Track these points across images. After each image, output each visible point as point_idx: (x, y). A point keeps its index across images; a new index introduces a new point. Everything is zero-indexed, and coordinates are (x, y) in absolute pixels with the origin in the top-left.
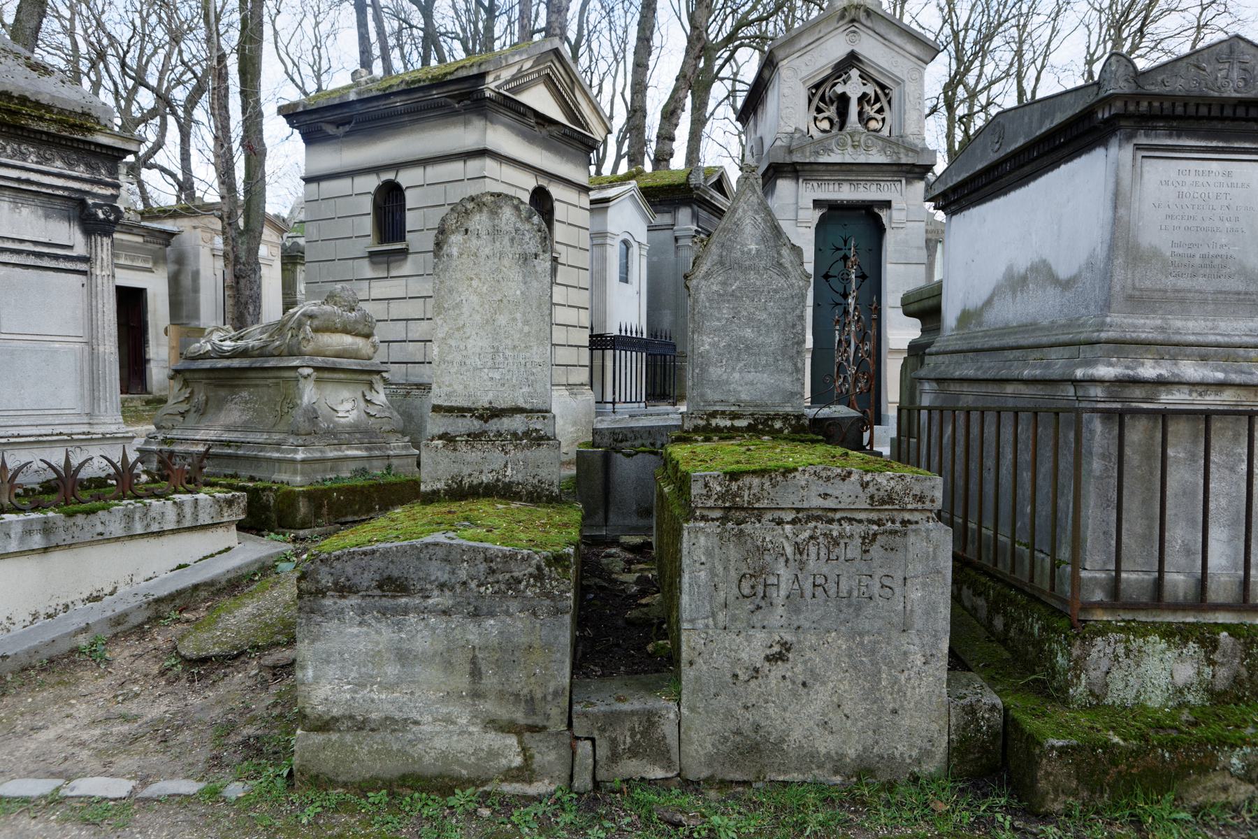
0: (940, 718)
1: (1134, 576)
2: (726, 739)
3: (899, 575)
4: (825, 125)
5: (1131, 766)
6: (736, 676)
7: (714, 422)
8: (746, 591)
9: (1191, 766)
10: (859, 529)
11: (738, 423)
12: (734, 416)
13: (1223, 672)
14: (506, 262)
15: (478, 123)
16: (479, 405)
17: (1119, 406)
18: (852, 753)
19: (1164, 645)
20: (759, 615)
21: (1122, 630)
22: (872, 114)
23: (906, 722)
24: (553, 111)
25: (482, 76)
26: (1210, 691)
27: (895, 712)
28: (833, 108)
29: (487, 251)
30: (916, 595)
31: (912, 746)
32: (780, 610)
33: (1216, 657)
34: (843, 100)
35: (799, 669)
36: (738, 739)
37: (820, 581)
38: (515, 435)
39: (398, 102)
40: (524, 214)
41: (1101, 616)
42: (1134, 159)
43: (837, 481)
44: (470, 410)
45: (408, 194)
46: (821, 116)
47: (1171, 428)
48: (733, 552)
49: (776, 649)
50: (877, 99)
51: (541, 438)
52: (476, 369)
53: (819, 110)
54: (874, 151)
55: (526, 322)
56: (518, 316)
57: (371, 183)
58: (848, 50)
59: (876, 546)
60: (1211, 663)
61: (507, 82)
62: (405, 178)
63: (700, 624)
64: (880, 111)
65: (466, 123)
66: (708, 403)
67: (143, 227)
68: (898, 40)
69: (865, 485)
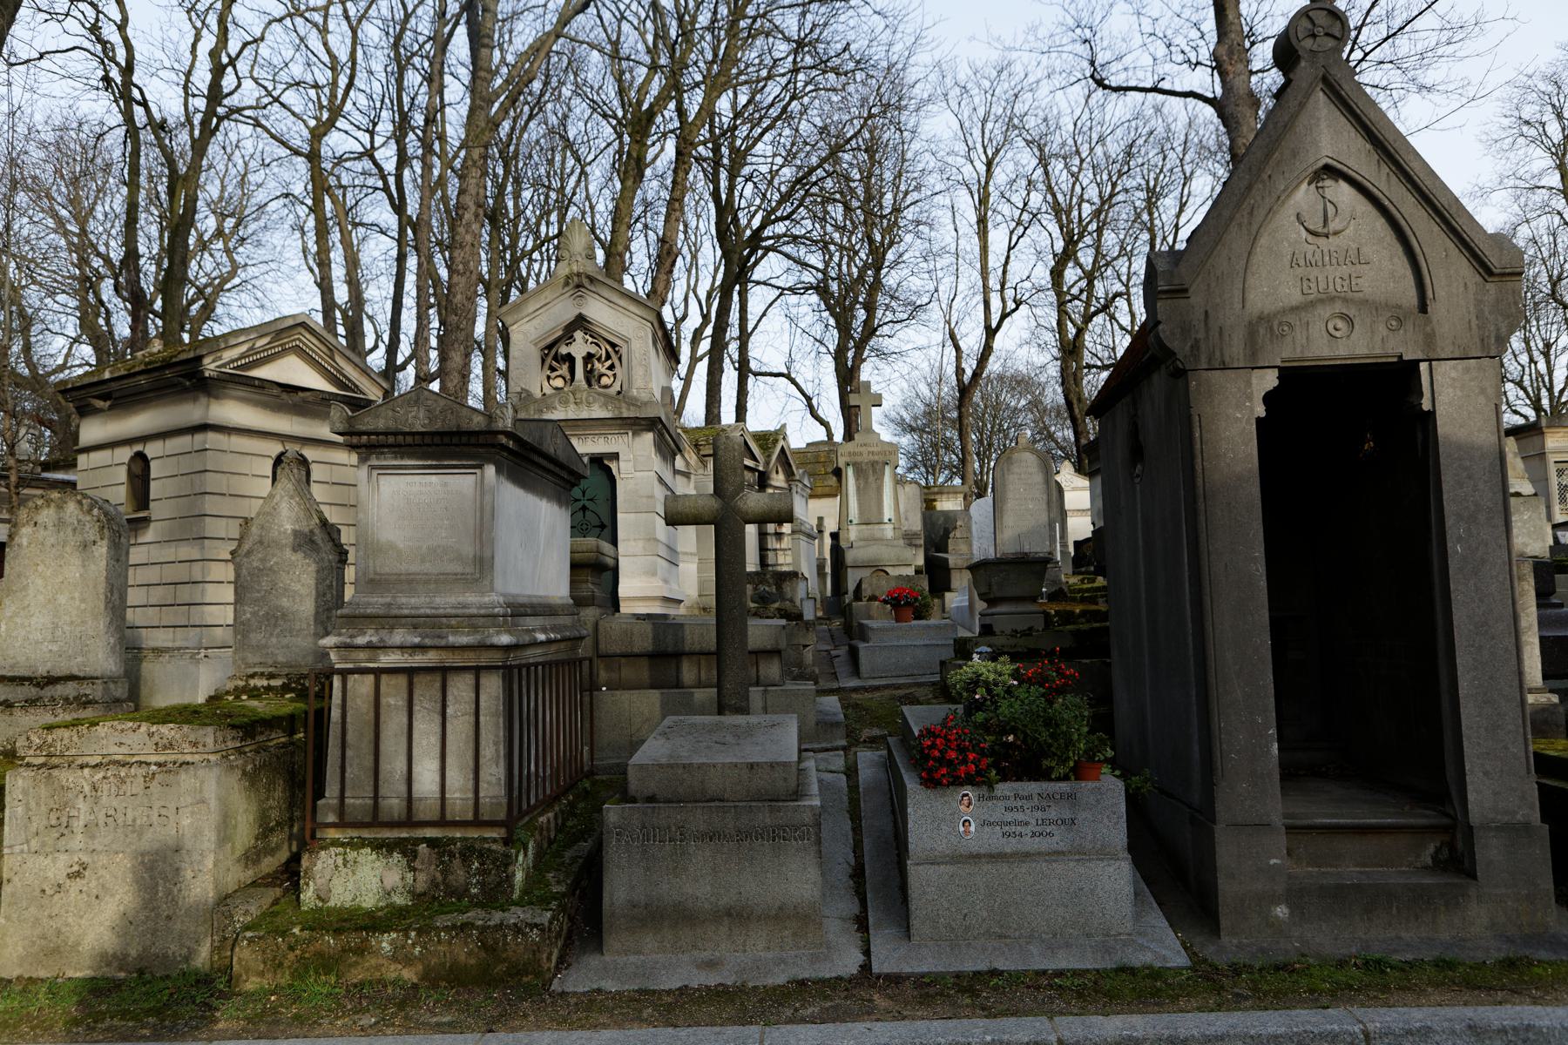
0: (205, 922)
1: (358, 802)
2: (34, 943)
3: (172, 806)
4: (559, 383)
5: (304, 952)
6: (43, 891)
7: (252, 682)
8: (54, 822)
9: (350, 950)
10: (142, 771)
11: (274, 683)
12: (271, 676)
13: (422, 877)
14: (68, 549)
15: (203, 400)
16: (38, 674)
17: (350, 666)
18: (133, 953)
19: (374, 856)
20: (63, 841)
21: (343, 845)
22: (603, 370)
23: (178, 926)
24: (312, 380)
25: (199, 358)
26: (412, 892)
27: (169, 918)
28: (565, 367)
29: (52, 540)
30: (186, 822)
31: (182, 946)
32: (80, 837)
33: (417, 864)
34: (570, 359)
35: (93, 884)
36: (43, 942)
37: (111, 812)
38: (66, 699)
39: (142, 380)
40: (86, 507)
41: (332, 834)
42: (370, 476)
43: (130, 733)
44: (30, 679)
45: (152, 464)
46: (553, 375)
47: (450, 683)
48: (43, 791)
49: (76, 868)
50: (608, 357)
51: (89, 702)
52: (37, 642)
53: (553, 369)
54: (596, 407)
55: (83, 600)
56: (77, 595)
57: (125, 454)
58: (576, 312)
59: (155, 783)
60: (414, 870)
61: (232, 361)
62: (151, 450)
63: (17, 849)
64: (611, 367)
65: (195, 400)
66: (248, 666)
67: (43, 479)
68: (622, 302)
69: (151, 735)
